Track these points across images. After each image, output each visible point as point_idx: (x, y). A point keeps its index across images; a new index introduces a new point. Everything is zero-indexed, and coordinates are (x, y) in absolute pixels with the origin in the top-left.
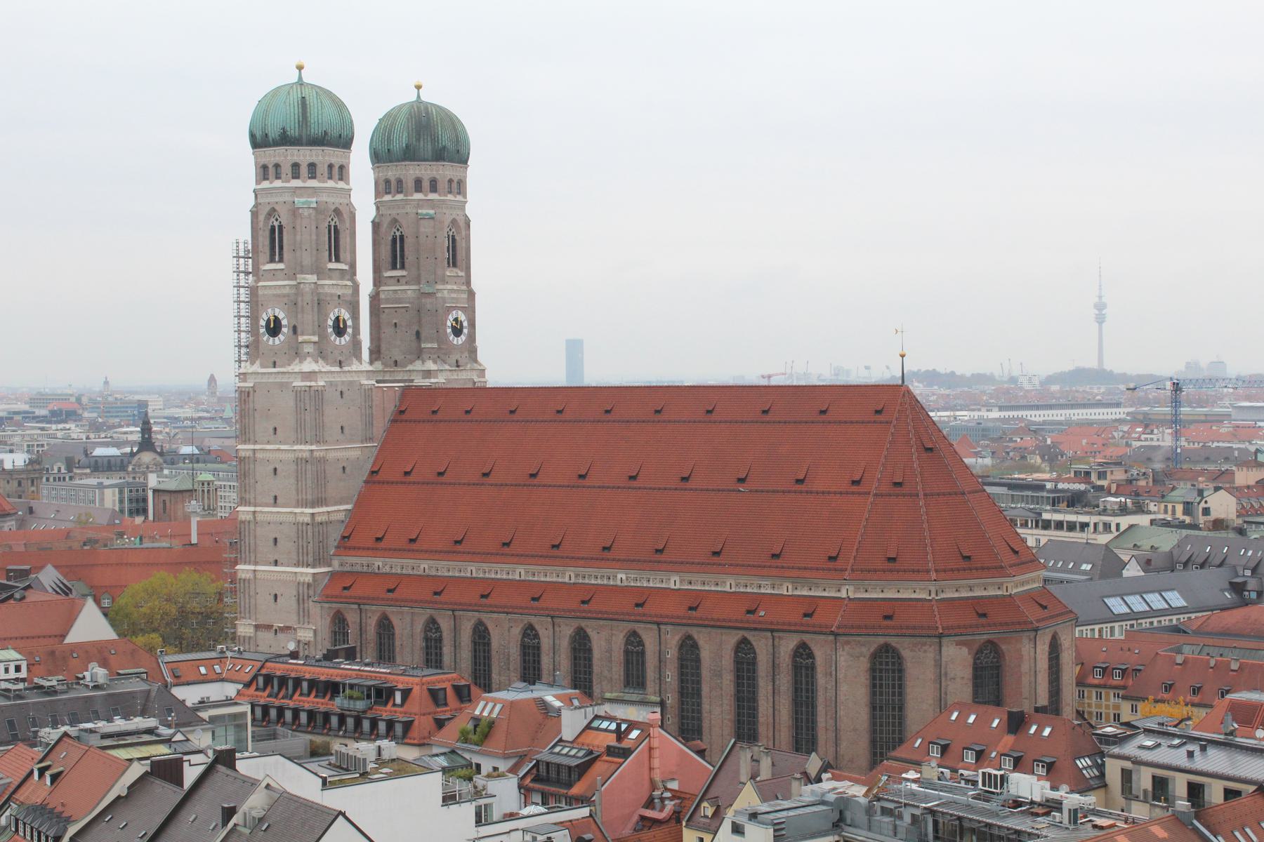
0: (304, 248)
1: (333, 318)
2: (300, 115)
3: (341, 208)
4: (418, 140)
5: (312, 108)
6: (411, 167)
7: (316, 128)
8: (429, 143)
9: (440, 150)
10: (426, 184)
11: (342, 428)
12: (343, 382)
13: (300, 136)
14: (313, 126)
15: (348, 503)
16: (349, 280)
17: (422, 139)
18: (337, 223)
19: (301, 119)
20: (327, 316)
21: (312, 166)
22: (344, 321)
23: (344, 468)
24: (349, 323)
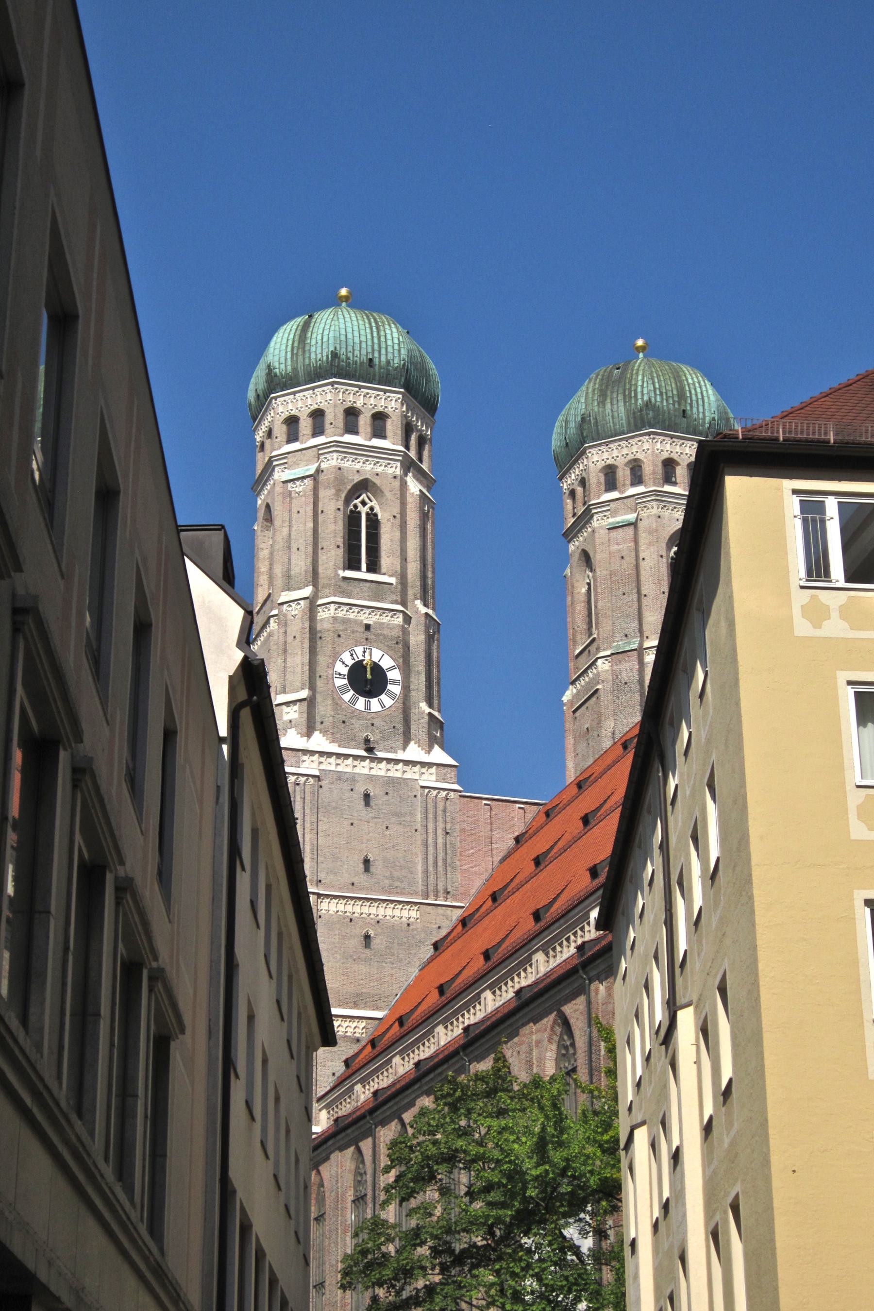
0: (294, 547)
1: (350, 662)
2: (297, 338)
3: (377, 481)
4: (602, 403)
5: (317, 325)
6: (593, 451)
7: (319, 351)
8: (621, 404)
9: (641, 410)
10: (623, 474)
11: (366, 862)
12: (371, 778)
13: (295, 369)
14: (313, 349)
15: (377, 1008)
16: (396, 602)
17: (609, 400)
18: (377, 510)
19: (296, 344)
20: (335, 656)
21: (318, 415)
22: (376, 668)
23: (367, 937)
24: (394, 675)
